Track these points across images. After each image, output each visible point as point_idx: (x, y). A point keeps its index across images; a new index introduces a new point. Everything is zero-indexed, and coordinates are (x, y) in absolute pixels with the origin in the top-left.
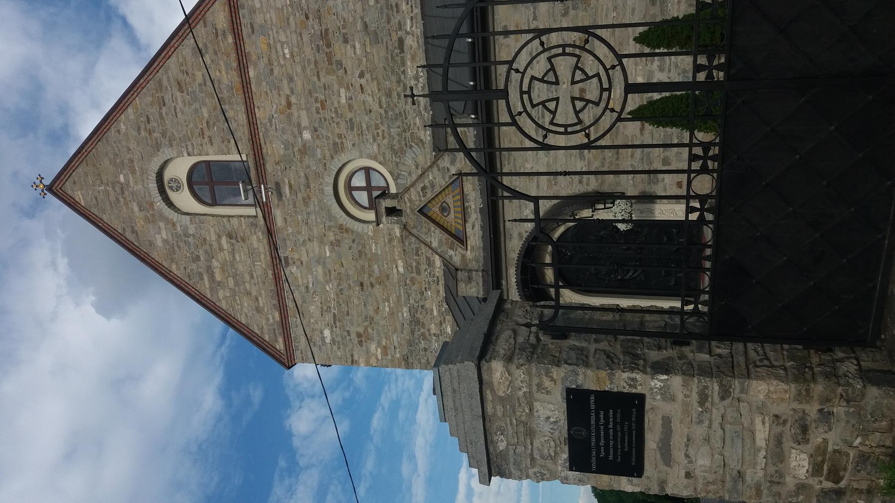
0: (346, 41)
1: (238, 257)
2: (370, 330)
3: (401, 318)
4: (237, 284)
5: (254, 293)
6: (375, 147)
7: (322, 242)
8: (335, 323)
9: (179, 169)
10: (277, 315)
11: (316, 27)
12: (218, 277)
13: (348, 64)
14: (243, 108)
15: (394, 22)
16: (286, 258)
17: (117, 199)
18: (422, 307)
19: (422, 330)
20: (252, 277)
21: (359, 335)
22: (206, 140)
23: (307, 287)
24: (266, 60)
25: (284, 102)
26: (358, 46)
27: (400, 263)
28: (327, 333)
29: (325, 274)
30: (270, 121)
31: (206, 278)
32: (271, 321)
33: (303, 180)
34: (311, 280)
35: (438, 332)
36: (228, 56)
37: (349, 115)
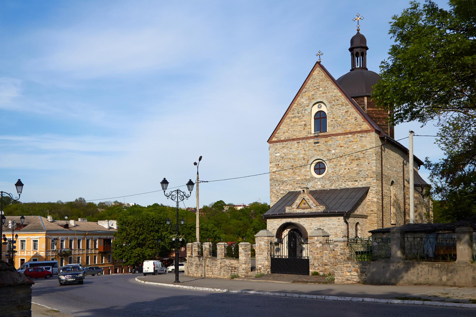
0: (357, 165)
4: (292, 126)
5: (289, 131)
6: (330, 172)
9: (324, 108)
10: (283, 139)
12: (293, 120)
13: (352, 165)
15: (362, 179)
16: (299, 143)
17: (315, 87)
21: (278, 165)
25: (342, 145)
26: (356, 168)
27: (299, 178)
28: (278, 154)
31: (293, 115)
33: (321, 150)
37: (338, 165)
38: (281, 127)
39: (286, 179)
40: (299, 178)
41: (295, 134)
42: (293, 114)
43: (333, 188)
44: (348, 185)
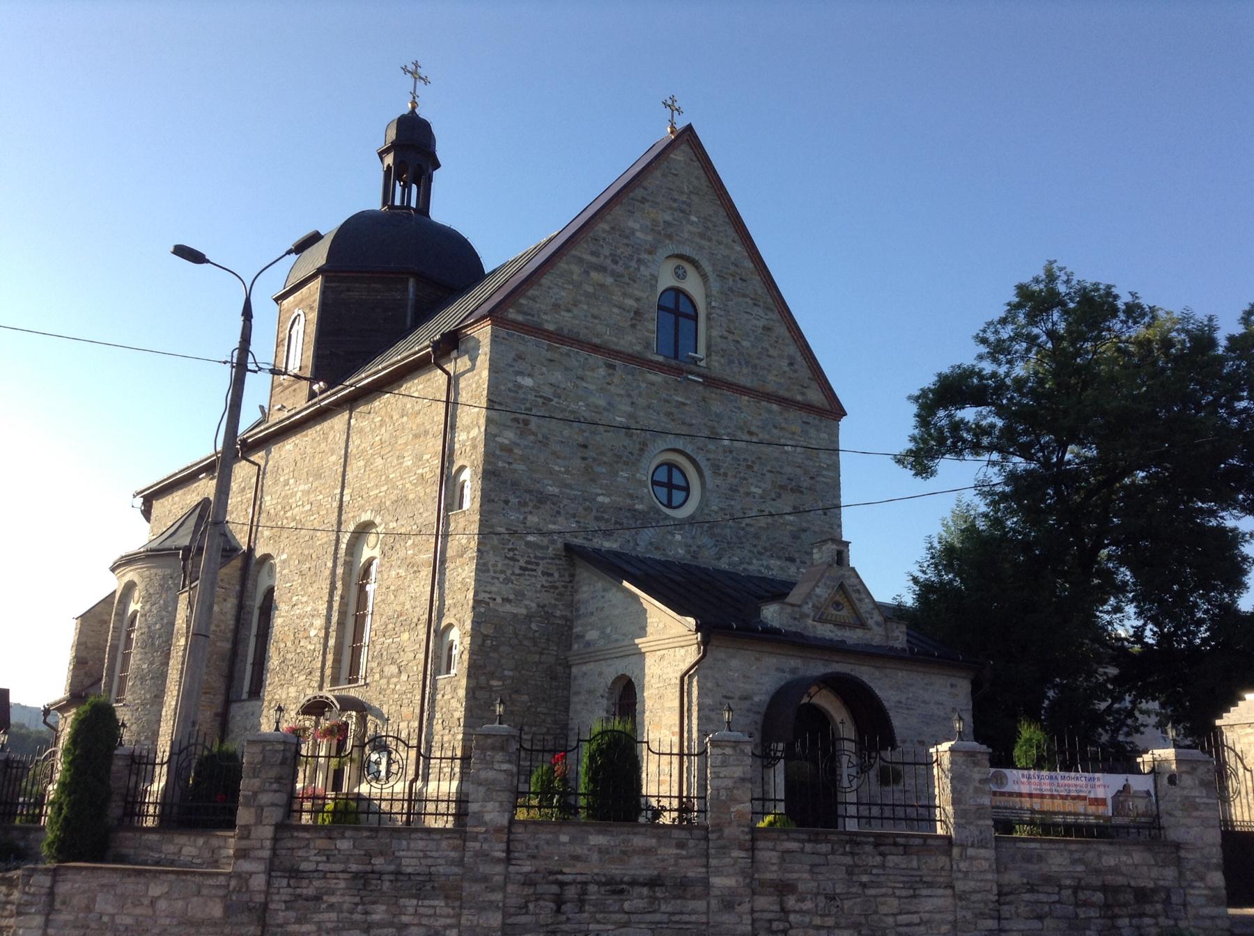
1: (616, 310)
2: (532, 438)
3: (546, 482)
4: (587, 295)
5: (575, 311)
6: (715, 508)
7: (631, 416)
8: (541, 397)
9: (692, 285)
10: (551, 327)
11: (805, 484)
14: (749, 385)
17: (675, 200)
18: (558, 512)
19: (531, 504)
20: (594, 317)
21: (526, 423)
22: (726, 334)
23: (582, 379)
24: (783, 425)
25: (753, 429)
27: (607, 500)
29: (596, 407)
30: (739, 408)
31: (593, 259)
32: (544, 317)
33: (688, 420)
34: (592, 387)
35: (528, 524)
36: (788, 390)
37: (742, 490)
38: (543, 281)
39: (555, 490)
40: (607, 500)
41: (600, 328)
42: (592, 253)
43: (723, 565)
44: (768, 567)
